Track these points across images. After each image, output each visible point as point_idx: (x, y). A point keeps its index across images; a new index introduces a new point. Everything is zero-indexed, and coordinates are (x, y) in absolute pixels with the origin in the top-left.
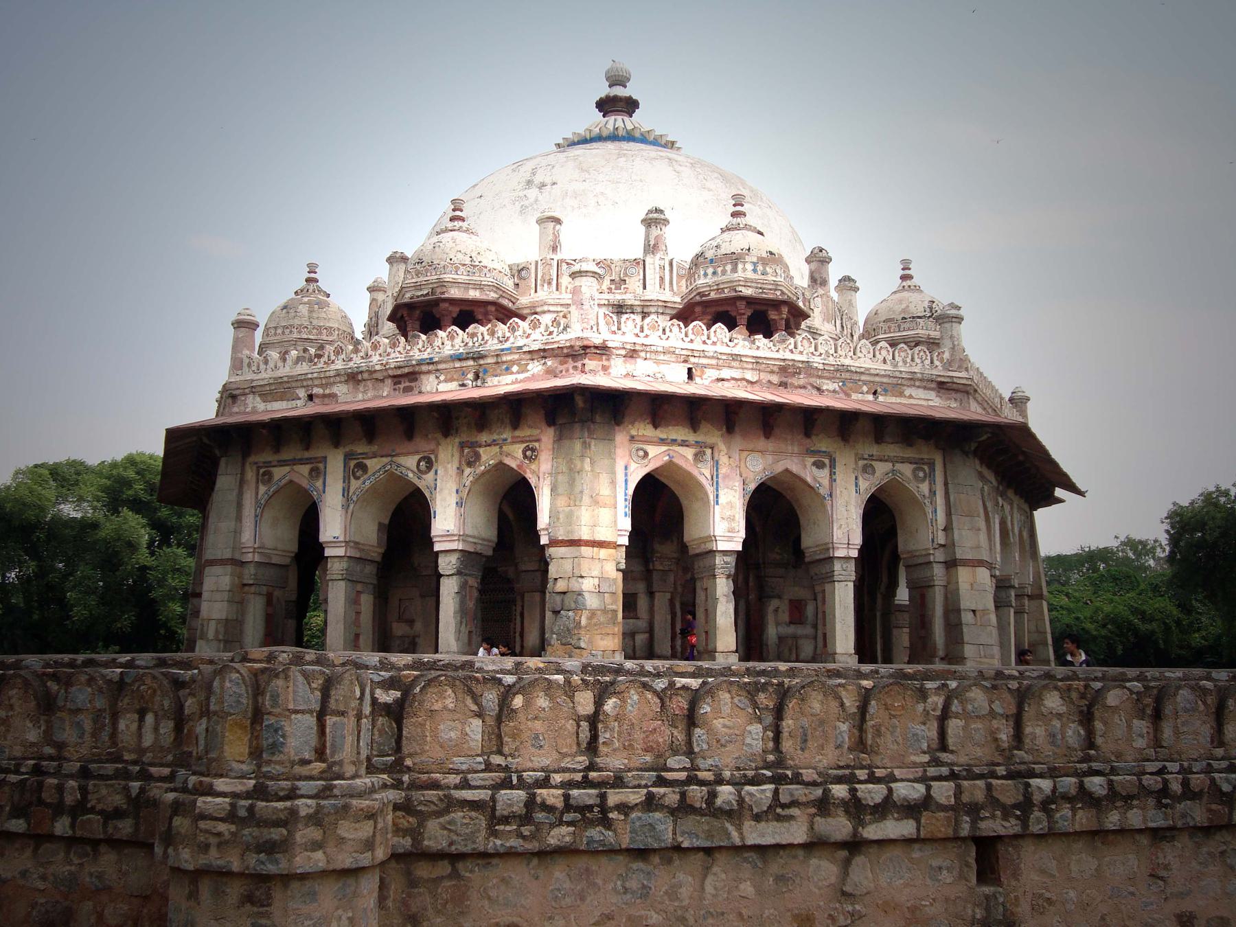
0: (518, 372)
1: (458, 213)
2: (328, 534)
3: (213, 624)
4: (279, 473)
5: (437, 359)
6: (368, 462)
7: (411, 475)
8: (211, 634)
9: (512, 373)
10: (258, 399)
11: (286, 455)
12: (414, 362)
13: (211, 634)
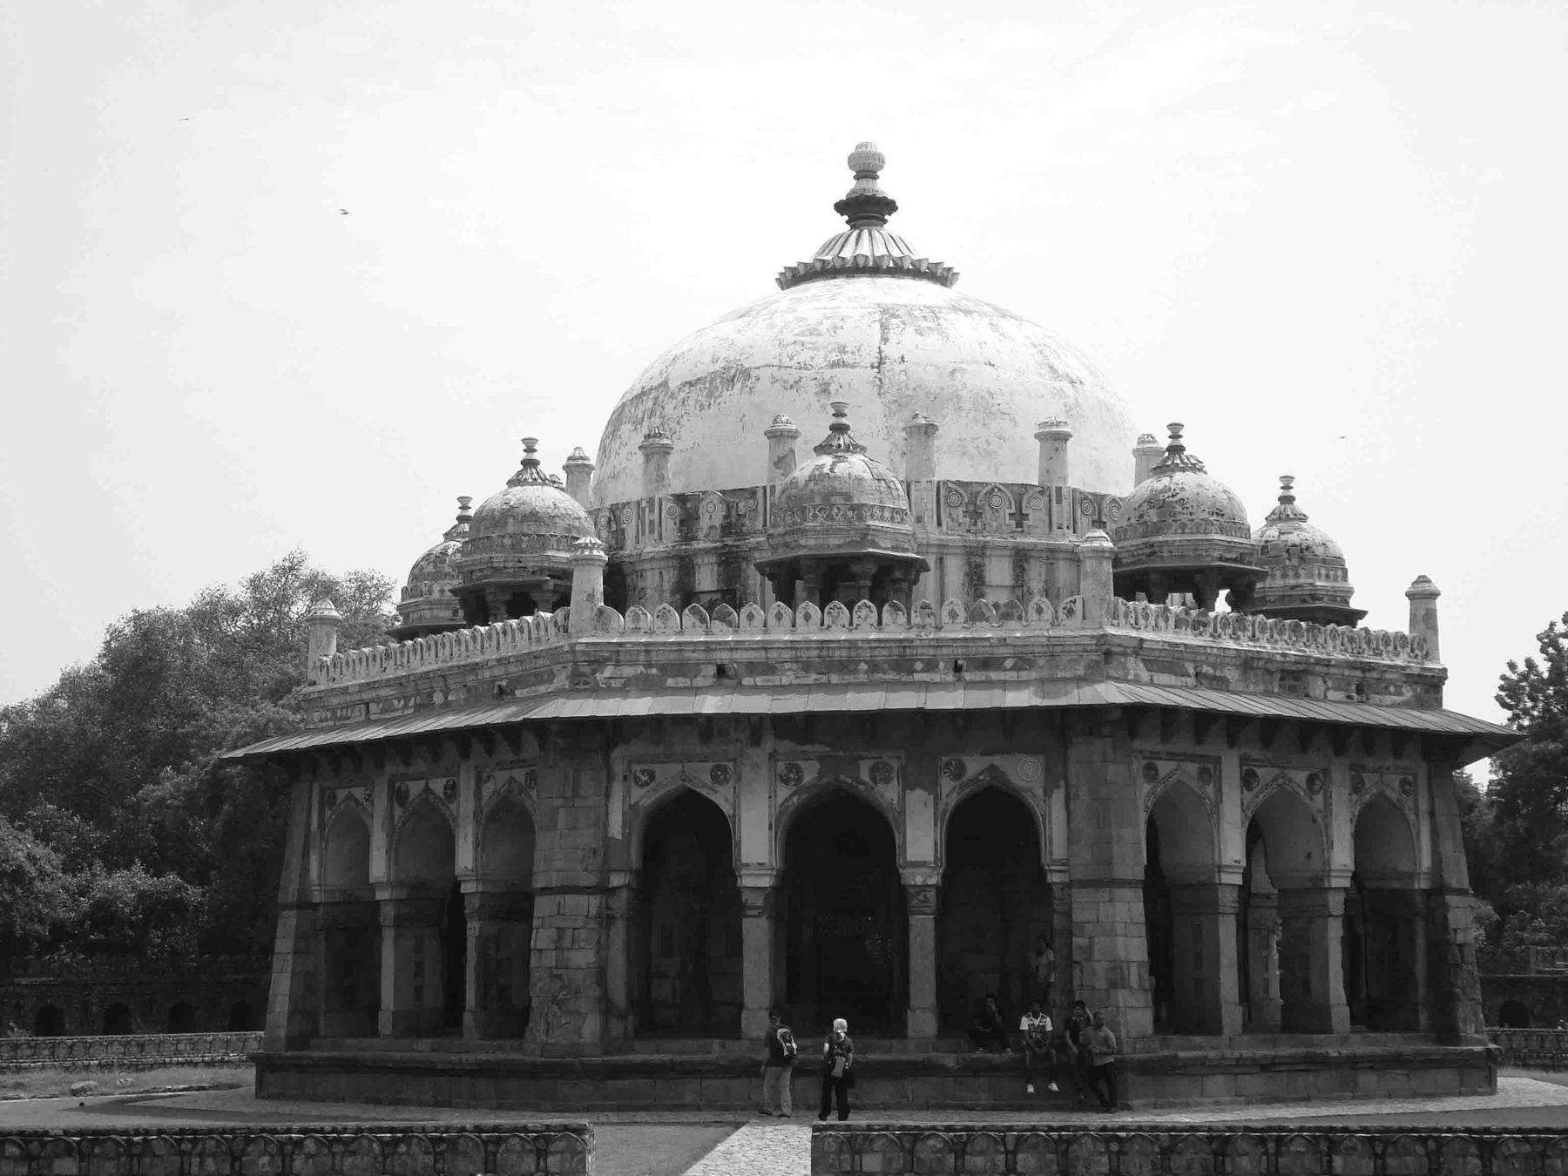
0: (1394, 694)
1: (1176, 443)
2: (1228, 856)
3: (1134, 967)
4: (1164, 767)
5: (1333, 662)
6: (1259, 771)
7: (1302, 794)
8: (1134, 983)
9: (1390, 694)
10: (1141, 665)
11: (1178, 745)
12: (1312, 660)
13: (1134, 983)
